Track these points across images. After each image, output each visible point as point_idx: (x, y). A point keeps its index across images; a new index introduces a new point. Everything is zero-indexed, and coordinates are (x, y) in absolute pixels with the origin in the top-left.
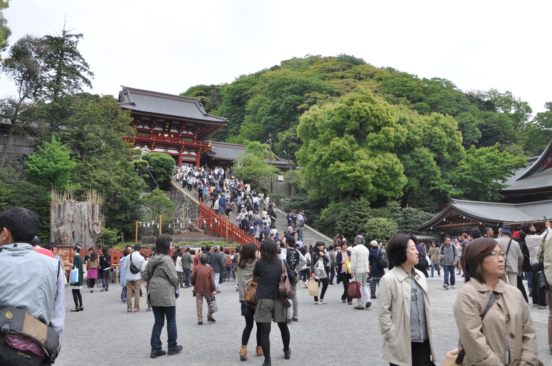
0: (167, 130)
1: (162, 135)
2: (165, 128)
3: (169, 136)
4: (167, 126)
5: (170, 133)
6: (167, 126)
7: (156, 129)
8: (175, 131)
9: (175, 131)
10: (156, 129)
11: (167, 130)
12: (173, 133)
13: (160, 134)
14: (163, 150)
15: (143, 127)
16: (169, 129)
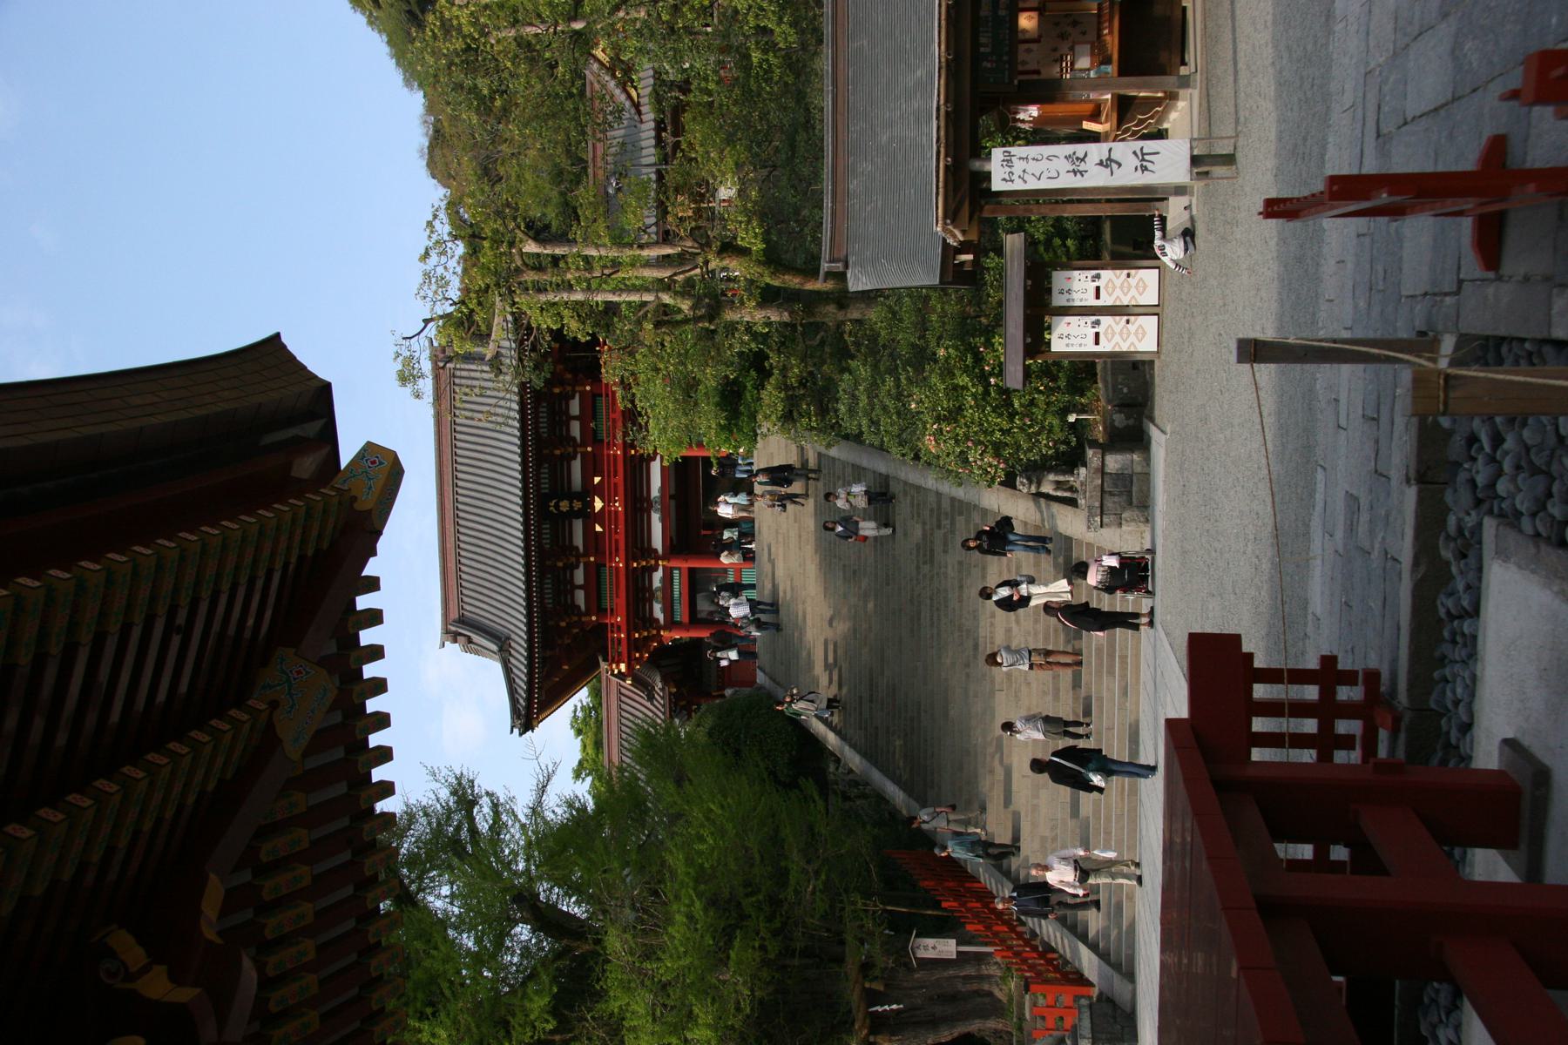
0: (577, 505)
1: (600, 517)
2: (573, 514)
3: (598, 491)
4: (564, 506)
5: (589, 491)
6: (564, 506)
7: (579, 541)
8: (577, 466)
9: (577, 466)
10: (579, 541)
11: (577, 505)
12: (586, 478)
13: (598, 528)
14: (656, 518)
15: (580, 587)
16: (571, 496)
